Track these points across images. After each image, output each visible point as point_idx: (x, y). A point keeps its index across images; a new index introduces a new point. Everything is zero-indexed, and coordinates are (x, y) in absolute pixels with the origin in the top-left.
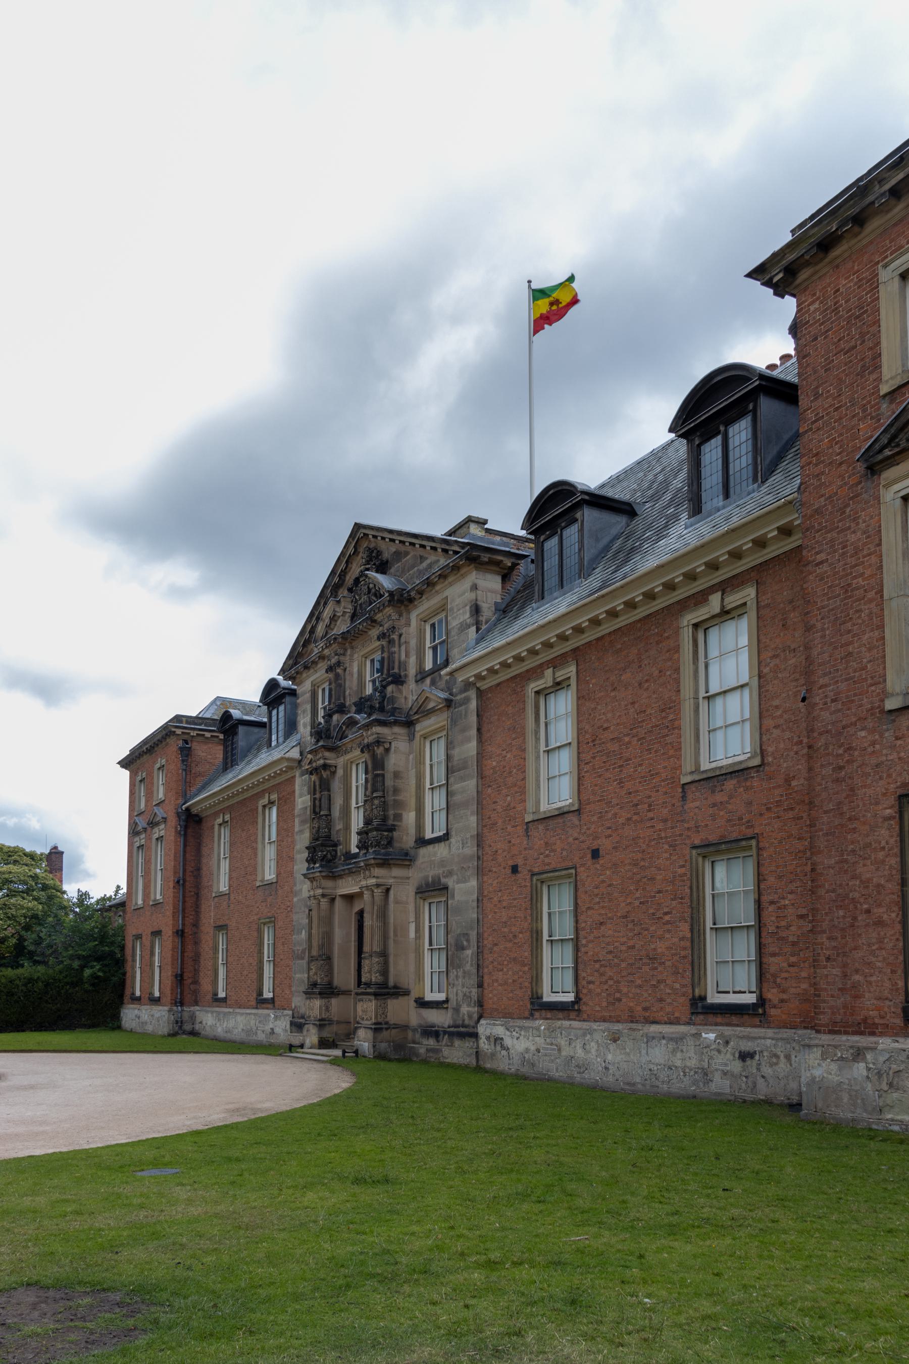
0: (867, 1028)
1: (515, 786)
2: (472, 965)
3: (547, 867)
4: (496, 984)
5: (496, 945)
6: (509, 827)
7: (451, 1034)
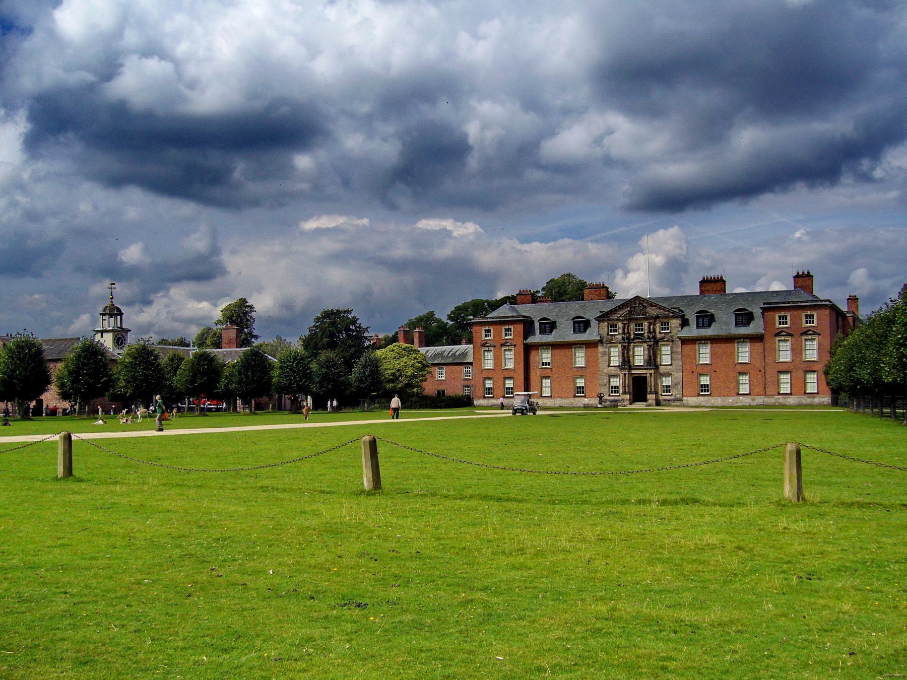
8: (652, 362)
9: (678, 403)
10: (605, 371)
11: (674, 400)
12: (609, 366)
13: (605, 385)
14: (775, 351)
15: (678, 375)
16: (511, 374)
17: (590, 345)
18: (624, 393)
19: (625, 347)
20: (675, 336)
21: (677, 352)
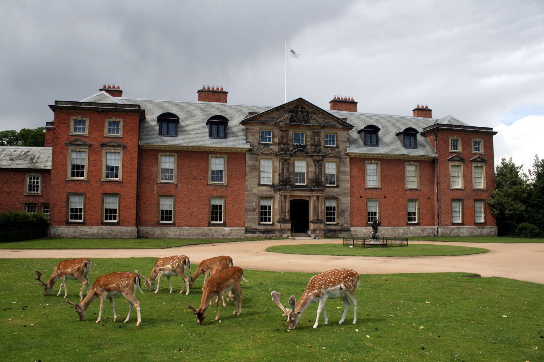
0: (447, 225)
9: (344, 234)
10: (255, 191)
12: (259, 185)
13: (254, 210)
14: (448, 177)
16: (117, 189)
17: (234, 157)
19: (286, 160)
20: (343, 153)
21: (345, 173)
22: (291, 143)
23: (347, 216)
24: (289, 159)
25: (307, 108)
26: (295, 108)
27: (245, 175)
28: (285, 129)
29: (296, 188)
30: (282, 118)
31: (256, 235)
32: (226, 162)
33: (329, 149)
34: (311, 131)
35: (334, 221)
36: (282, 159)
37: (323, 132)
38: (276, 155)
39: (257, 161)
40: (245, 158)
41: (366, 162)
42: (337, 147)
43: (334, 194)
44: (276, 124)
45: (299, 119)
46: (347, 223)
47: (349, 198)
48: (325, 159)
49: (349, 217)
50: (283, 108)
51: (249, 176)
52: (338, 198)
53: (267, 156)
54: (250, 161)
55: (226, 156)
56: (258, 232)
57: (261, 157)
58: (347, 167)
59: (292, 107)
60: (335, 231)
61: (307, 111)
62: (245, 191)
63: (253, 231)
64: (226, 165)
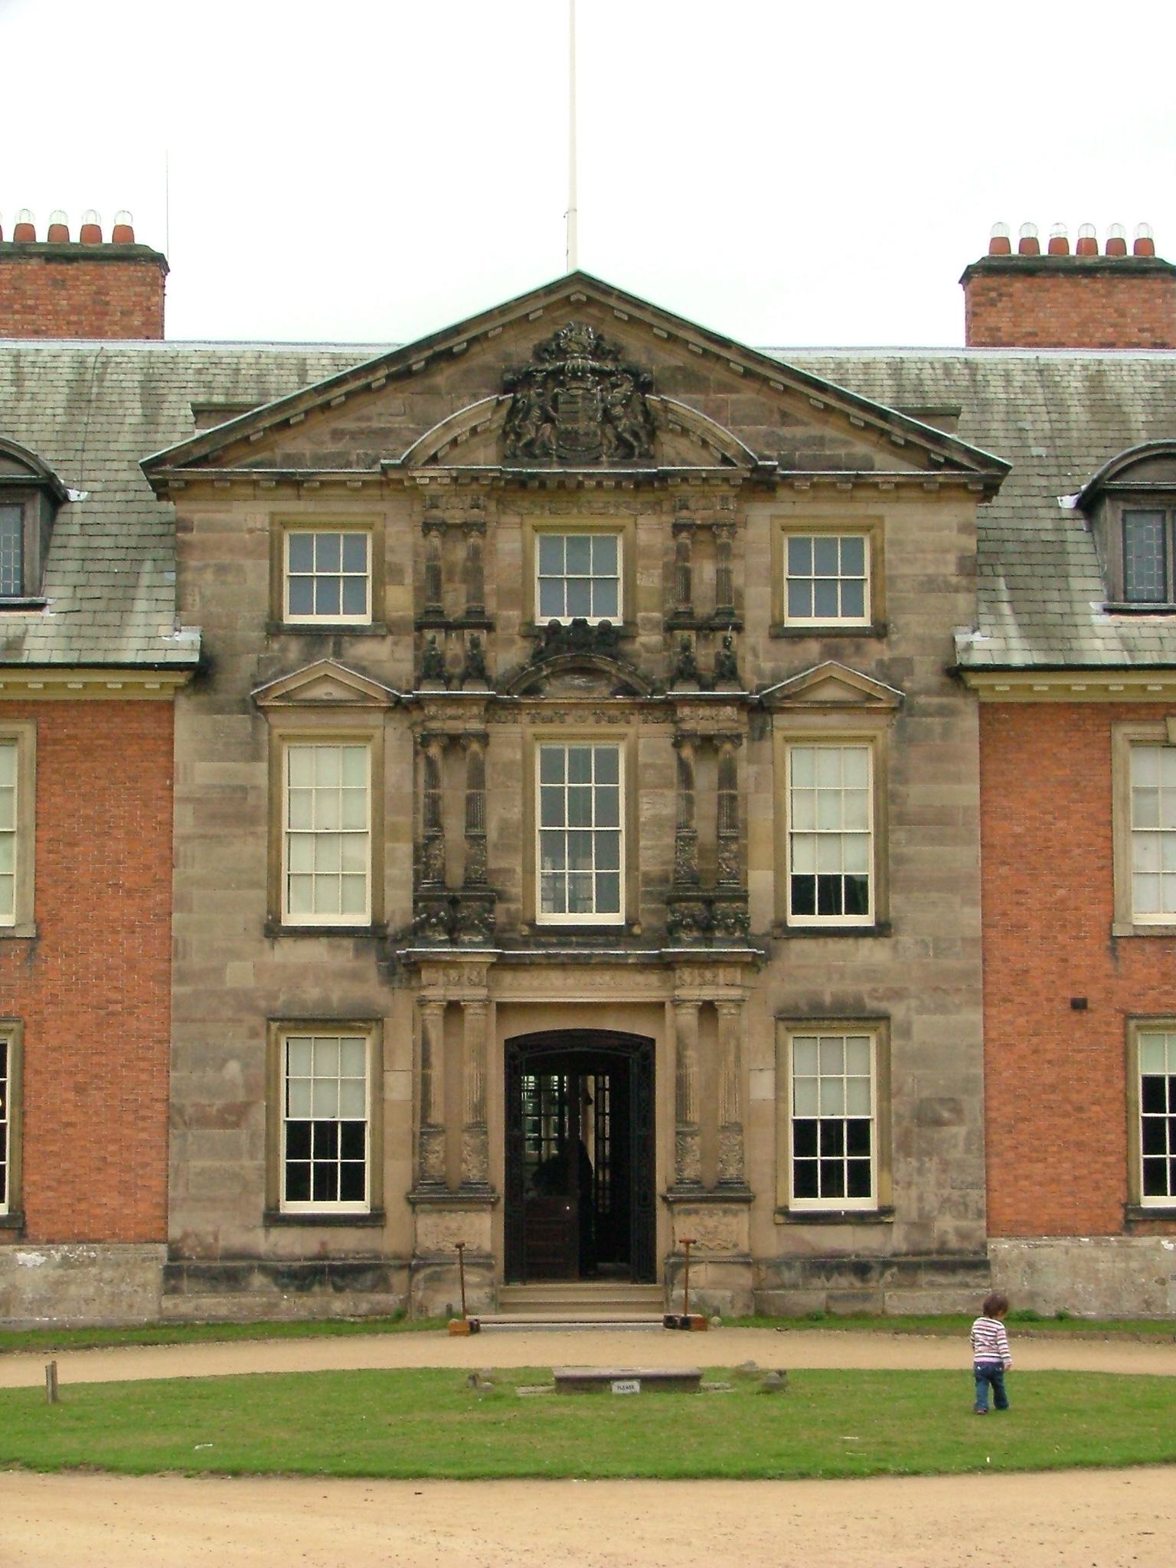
1: (1080, 874)
2: (968, 1151)
3: (1165, 1010)
4: (1023, 1183)
5: (1024, 1119)
6: (1060, 938)
7: (904, 1267)
8: (698, 909)
10: (239, 975)
11: (910, 1266)
12: (274, 930)
13: (234, 1115)
15: (949, 1033)
18: (435, 1193)
19: (454, 743)
21: (939, 822)
22: (514, 614)
23: (957, 1154)
24: (484, 738)
25: (637, 350)
26: (541, 352)
27: (169, 861)
28: (456, 516)
29: (522, 946)
30: (431, 437)
31: (246, 1300)
32: (31, 770)
33: (814, 647)
34: (668, 520)
35: (860, 1188)
36: (425, 741)
37: (760, 522)
38: (398, 706)
39: (255, 757)
40: (170, 740)
41: (1122, 733)
42: (880, 631)
43: (848, 988)
44: (390, 482)
45: (570, 437)
46: (962, 1208)
47: (976, 1016)
48: (780, 721)
49: (975, 1160)
50: (449, 356)
51: (196, 871)
52: (885, 1018)
53: (329, 717)
54: (210, 755)
55: (28, 731)
56: (258, 1280)
57: (283, 724)
58: (957, 778)
59: (521, 349)
60: (861, 1269)
61: (634, 373)
62: (165, 979)
63: (228, 1272)
64: (30, 798)
